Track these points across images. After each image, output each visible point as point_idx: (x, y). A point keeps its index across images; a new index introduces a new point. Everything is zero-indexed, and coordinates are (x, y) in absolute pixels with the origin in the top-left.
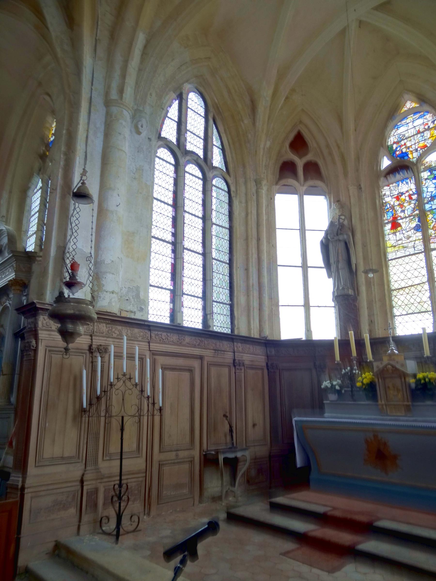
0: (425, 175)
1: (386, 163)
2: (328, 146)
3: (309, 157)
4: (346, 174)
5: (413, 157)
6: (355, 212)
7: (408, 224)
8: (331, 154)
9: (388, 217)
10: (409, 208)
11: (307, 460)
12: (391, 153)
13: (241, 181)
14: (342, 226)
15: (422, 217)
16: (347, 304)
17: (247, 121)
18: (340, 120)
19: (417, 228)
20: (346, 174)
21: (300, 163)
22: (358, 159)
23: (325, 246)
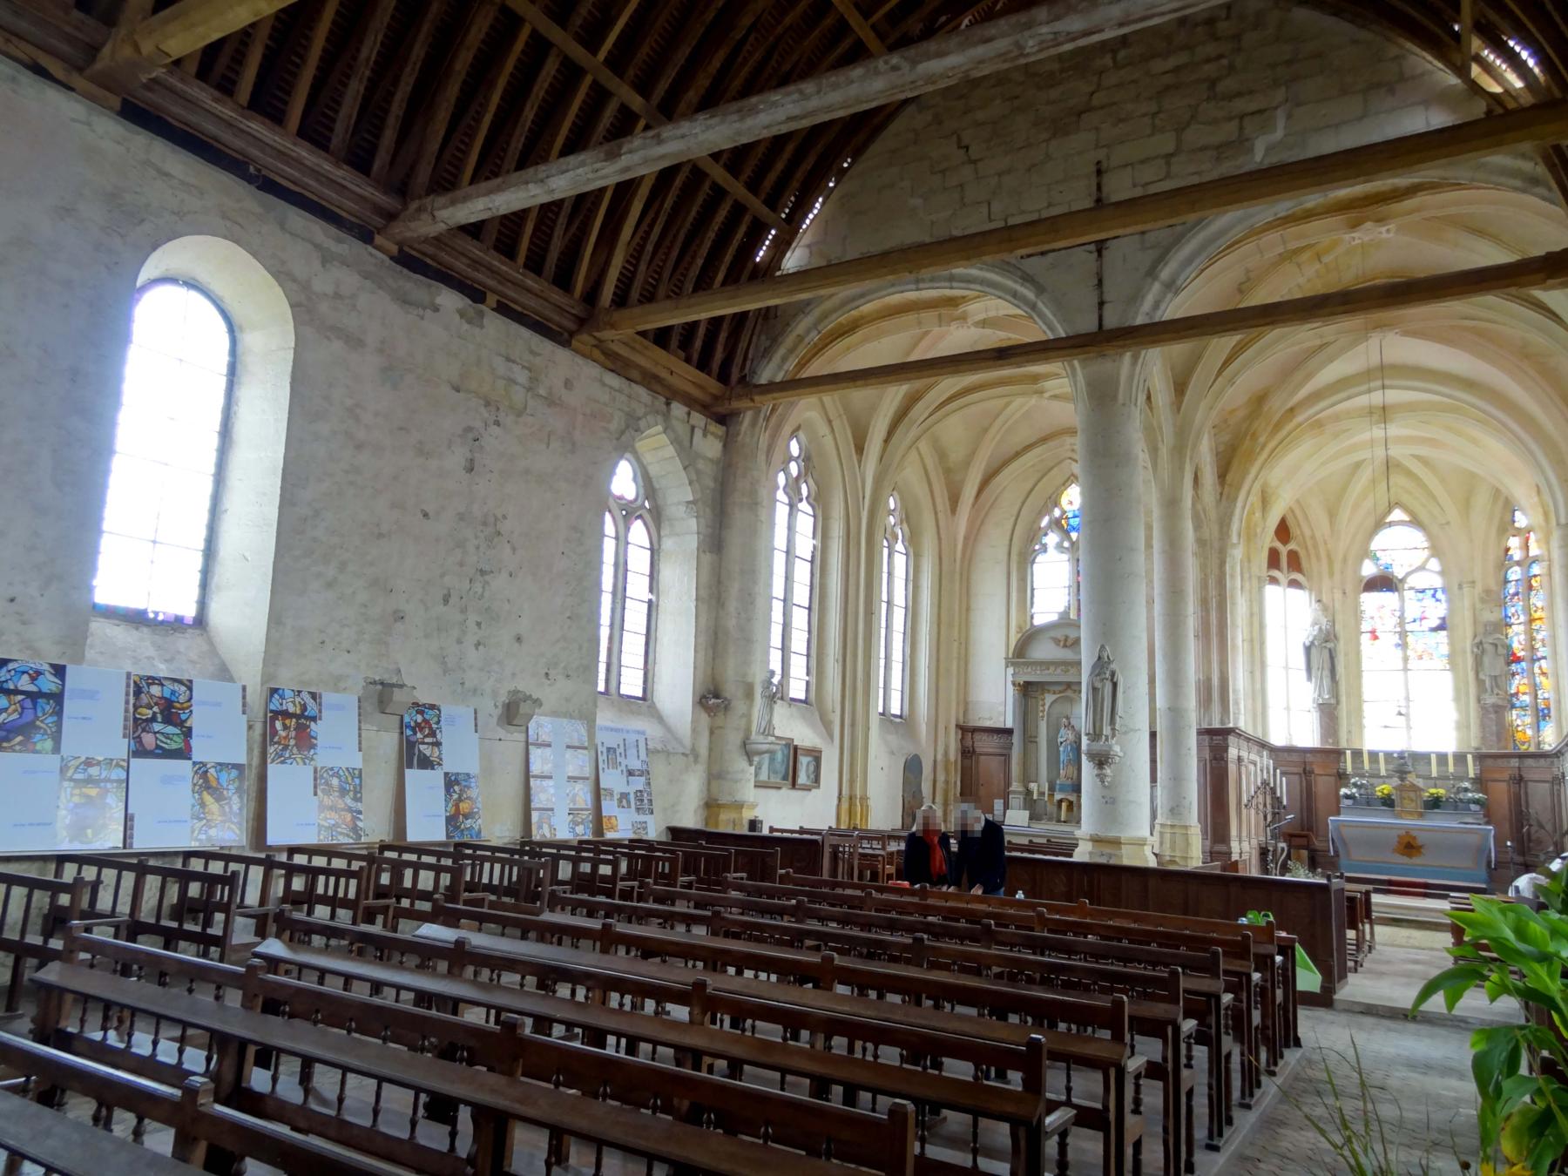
0: (1408, 594)
1: (1369, 569)
2: (1313, 537)
3: (1292, 546)
4: (1331, 574)
5: (1399, 573)
6: (1339, 618)
7: (1389, 639)
8: (1315, 546)
9: (1365, 626)
10: (1391, 622)
11: (1336, 851)
12: (1376, 559)
13: (1246, 576)
14: (1328, 633)
15: (1403, 634)
16: (1329, 714)
17: (1258, 515)
18: (1332, 515)
19: (1398, 645)
20: (1331, 574)
21: (1284, 551)
22: (1345, 560)
23: (1308, 650)
